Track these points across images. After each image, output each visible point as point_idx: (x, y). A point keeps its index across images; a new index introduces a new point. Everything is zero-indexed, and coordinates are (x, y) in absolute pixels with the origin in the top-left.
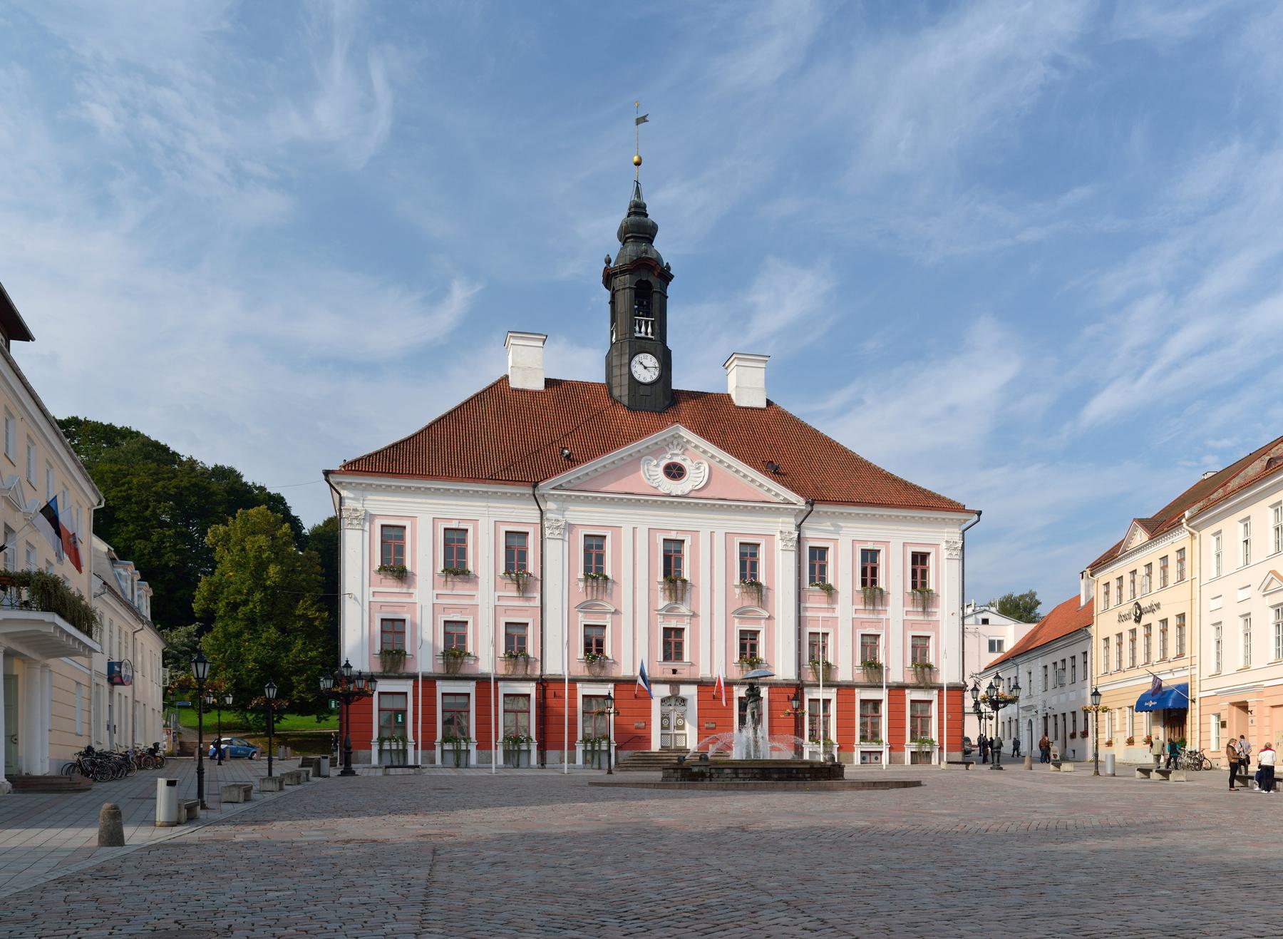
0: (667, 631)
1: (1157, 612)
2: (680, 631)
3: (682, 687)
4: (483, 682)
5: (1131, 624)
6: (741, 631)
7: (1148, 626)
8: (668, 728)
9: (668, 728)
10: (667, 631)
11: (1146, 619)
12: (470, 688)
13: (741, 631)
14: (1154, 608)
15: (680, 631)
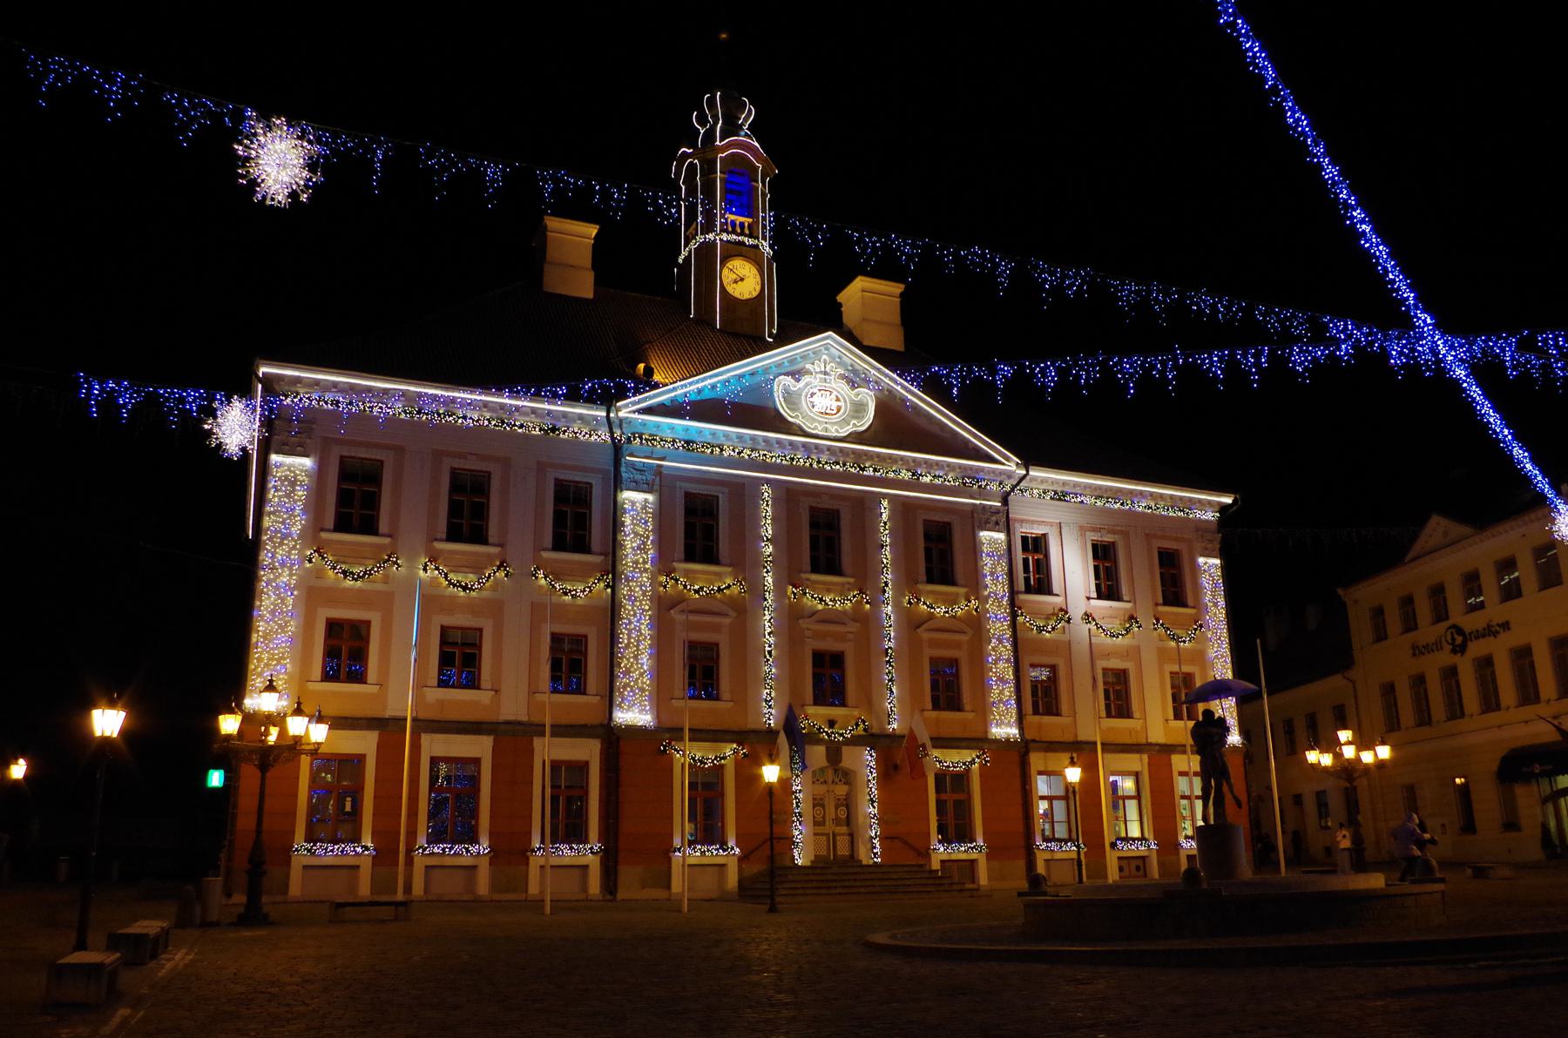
0: (819, 658)
1: (1503, 636)
2: (837, 660)
3: (845, 749)
4: (513, 738)
5: (1445, 657)
6: (933, 661)
7: (1486, 663)
8: (822, 823)
9: (822, 823)
10: (819, 658)
11: (1477, 649)
12: (479, 747)
13: (933, 661)
14: (1490, 631)
15: (837, 660)
